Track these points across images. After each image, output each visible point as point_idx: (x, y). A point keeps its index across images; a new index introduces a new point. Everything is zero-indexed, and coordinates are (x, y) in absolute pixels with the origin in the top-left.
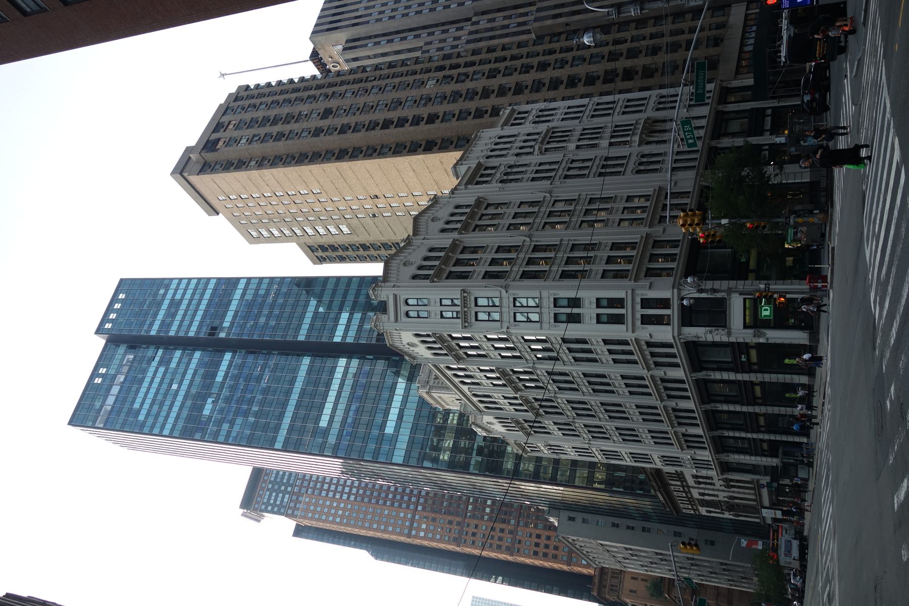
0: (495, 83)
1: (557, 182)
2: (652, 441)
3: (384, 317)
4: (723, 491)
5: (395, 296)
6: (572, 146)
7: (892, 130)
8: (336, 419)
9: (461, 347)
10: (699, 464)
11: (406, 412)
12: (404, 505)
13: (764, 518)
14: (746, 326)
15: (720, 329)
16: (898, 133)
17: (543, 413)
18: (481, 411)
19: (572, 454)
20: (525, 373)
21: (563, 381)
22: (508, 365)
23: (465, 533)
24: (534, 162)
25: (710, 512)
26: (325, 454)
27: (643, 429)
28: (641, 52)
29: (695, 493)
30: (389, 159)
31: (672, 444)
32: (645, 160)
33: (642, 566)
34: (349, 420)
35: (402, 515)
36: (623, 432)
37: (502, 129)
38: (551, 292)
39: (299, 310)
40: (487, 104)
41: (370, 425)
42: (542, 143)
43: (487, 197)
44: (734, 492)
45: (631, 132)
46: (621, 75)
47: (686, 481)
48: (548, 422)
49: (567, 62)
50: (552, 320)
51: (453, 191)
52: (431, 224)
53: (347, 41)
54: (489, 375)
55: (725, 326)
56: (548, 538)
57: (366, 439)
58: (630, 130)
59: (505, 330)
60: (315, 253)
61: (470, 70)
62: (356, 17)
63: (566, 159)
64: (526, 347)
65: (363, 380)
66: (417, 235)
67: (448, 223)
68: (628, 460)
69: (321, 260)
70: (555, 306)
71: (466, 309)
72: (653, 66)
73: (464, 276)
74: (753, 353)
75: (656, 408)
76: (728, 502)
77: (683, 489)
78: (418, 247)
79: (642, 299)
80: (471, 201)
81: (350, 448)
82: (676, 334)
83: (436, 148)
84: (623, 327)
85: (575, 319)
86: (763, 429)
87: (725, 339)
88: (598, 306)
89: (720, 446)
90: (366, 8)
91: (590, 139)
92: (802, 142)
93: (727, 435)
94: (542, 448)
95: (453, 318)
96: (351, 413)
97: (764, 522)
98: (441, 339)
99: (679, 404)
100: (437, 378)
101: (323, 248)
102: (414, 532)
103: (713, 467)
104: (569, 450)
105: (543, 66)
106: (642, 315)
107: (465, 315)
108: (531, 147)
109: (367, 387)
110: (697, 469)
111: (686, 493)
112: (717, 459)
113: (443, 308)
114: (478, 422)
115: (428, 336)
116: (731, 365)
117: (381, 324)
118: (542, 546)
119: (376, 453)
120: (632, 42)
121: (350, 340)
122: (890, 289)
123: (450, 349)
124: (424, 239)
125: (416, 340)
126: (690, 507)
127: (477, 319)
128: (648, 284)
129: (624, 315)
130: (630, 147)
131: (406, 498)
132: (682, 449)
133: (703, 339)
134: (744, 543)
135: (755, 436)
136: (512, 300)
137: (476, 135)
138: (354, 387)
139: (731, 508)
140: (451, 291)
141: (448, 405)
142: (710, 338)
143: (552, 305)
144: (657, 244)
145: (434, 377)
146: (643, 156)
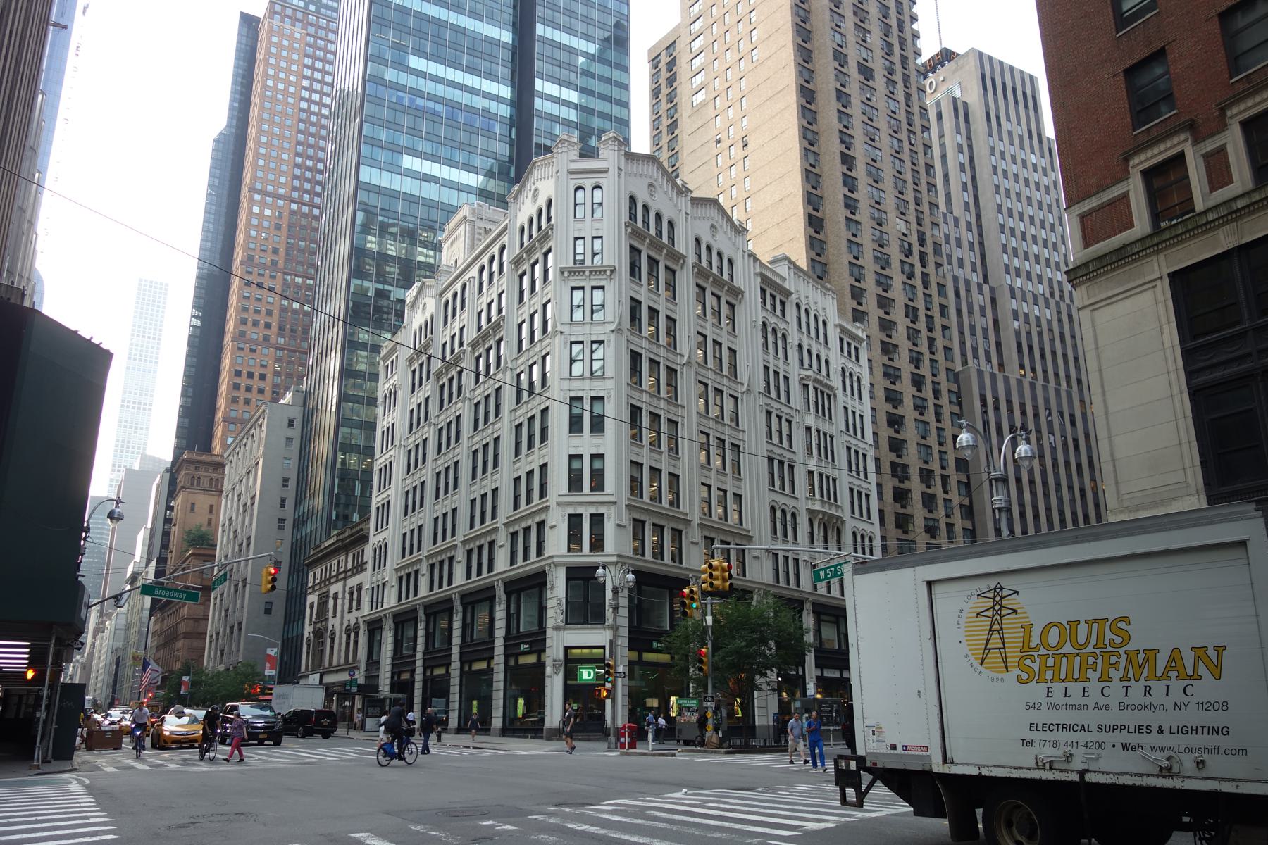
0: (898, 315)
1: (762, 401)
2: (407, 530)
3: (575, 153)
4: (342, 624)
5: (605, 171)
6: (810, 421)
7: (843, 819)
8: (421, 81)
9: (533, 266)
10: (378, 592)
11: (435, 187)
12: (296, 183)
13: (308, 676)
14: (567, 649)
15: (563, 617)
16: (840, 828)
17: (441, 383)
18: (441, 294)
19: (385, 423)
20: (498, 358)
21: (487, 410)
22: (509, 333)
23: (262, 272)
24: (790, 369)
25: (312, 608)
26: (369, 63)
27: (424, 518)
28: (931, 511)
29: (336, 588)
30: (799, 163)
31: (403, 556)
32: (789, 517)
33: (230, 519)
34: (420, 102)
35: (283, 180)
36: (418, 491)
37: (836, 326)
38: (613, 393)
39: (581, 27)
40: (870, 305)
41: (414, 132)
42: (816, 380)
43: (743, 302)
44: (341, 637)
45: (825, 499)
46: (901, 485)
47: (353, 575)
48: (429, 389)
49: (922, 414)
50: (573, 394)
51: (752, 255)
52: (708, 224)
53: (965, 104)
54: (494, 306)
55: (567, 623)
56: (261, 391)
57: (394, 126)
58: (829, 498)
59: (559, 329)
60: (664, 53)
61: (918, 281)
62: (998, 118)
63: (793, 413)
64: (535, 359)
65: (479, 122)
66: (692, 204)
67: (709, 248)
68: (379, 498)
69: (655, 62)
70: (593, 398)
71: (587, 273)
72: (911, 527)
73: (634, 270)
74: (532, 659)
75: (453, 535)
76: (326, 629)
78: (676, 206)
79: (602, 515)
80: (739, 282)
81: (379, 102)
82: (555, 560)
83: (812, 232)
84: (564, 488)
85: (575, 425)
86: (428, 673)
87: (550, 623)
88: (593, 457)
89: (404, 620)
90: (1010, 133)
91: (819, 445)
92: (807, 715)
93: (419, 627)
94: (391, 382)
95: (575, 254)
96: (430, 104)
97: (301, 677)
98: (544, 237)
99: (460, 565)
100: (487, 231)
101: (672, 64)
102: (257, 197)
103: (374, 611)
104: (390, 419)
105: (918, 382)
106: (581, 515)
107: (579, 272)
108: (811, 366)
109: (470, 128)
111: (336, 576)
112: (385, 615)
113: (588, 240)
114: (425, 291)
115: (549, 219)
116: (515, 632)
117: (565, 150)
118: (249, 382)
119: (374, 142)
120: (945, 500)
121: (538, 103)
122: (639, 821)
123: (530, 250)
124: (687, 214)
125: (542, 202)
126: (317, 581)
127: (573, 288)
128: (623, 523)
129: (582, 490)
130: (807, 498)
131: (307, 186)
132: (397, 570)
133: (549, 595)
134: (273, 652)
135: (419, 663)
136: (601, 338)
137: (828, 289)
138: (470, 109)
139: (319, 634)
140: (613, 253)
141: (449, 247)
142: (550, 604)
143: (594, 394)
144: (677, 534)
145: (488, 228)
146: (794, 515)
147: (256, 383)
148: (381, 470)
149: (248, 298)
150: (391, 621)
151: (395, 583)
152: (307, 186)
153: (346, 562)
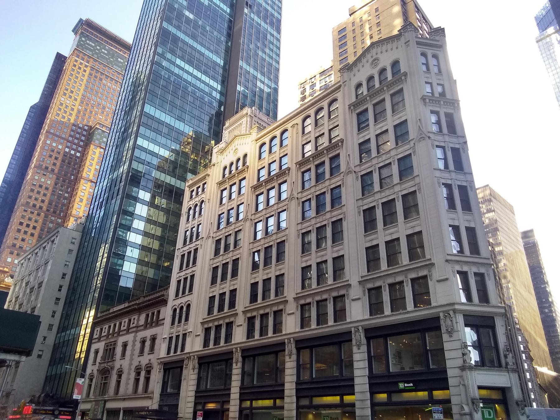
4: (131, 364)
12: (72, 133)
23: (45, 173)
26: (156, 56)
29: (129, 338)
33: (17, 298)
35: (65, 130)
44: (129, 374)
56: (32, 235)
77: (133, 328)
82: (457, 307)
102: (50, 136)
107: (436, 101)
118: (27, 229)
131: (78, 136)
147: (30, 230)
148: (183, 256)
149: (35, 185)
150: (196, 361)
151: (200, 331)
152: (78, 136)
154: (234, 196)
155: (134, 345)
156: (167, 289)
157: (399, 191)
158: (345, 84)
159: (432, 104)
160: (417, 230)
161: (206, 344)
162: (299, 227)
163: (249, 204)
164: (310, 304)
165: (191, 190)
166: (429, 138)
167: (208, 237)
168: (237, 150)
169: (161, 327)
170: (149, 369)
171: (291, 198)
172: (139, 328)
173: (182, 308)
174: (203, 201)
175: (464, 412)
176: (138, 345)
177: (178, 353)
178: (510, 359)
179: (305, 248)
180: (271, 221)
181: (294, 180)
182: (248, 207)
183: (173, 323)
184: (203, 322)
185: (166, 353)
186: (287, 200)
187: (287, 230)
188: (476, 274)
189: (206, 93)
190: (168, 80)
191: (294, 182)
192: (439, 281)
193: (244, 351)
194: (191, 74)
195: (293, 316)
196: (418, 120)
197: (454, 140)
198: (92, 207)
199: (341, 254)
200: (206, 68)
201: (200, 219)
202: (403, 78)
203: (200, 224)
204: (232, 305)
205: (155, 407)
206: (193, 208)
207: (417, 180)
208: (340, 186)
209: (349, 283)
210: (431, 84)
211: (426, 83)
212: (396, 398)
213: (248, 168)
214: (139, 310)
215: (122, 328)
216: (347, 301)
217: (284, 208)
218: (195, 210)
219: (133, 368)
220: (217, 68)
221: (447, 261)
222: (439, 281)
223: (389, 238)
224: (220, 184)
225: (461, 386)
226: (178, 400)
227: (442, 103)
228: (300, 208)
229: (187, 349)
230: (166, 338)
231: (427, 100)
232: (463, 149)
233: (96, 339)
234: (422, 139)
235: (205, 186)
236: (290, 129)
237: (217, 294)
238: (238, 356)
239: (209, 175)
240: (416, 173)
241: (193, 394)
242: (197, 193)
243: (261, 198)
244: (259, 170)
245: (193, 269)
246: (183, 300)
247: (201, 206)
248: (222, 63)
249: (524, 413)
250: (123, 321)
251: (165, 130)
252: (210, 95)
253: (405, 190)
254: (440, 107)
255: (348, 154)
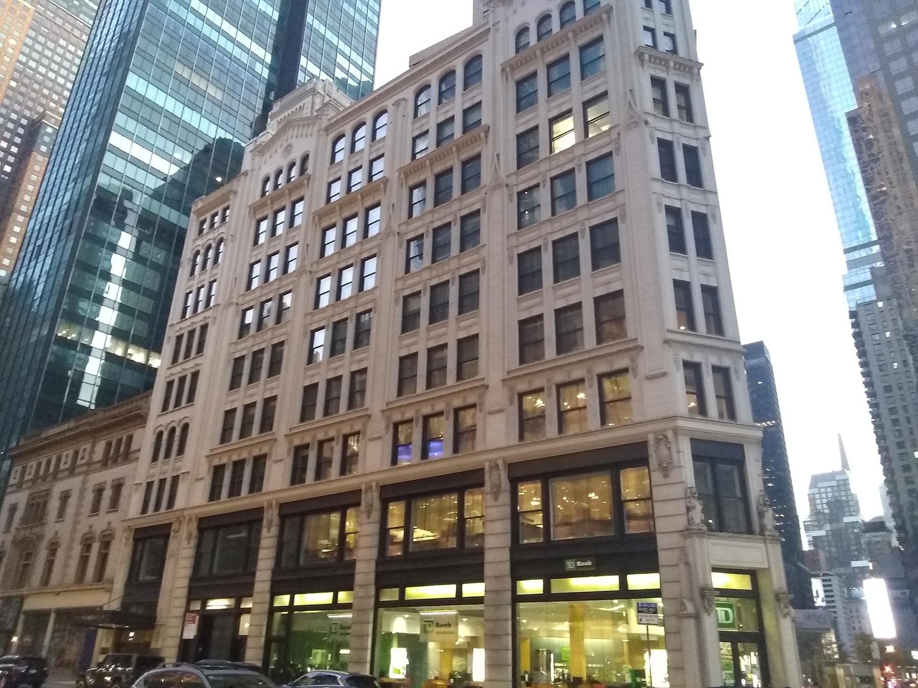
2: (321, 378)
4: (74, 531)
29: (73, 484)
77: (82, 465)
82: (681, 423)
110: (145, 485)
148: (179, 338)
151: (205, 472)
153: (92, 452)
154: (280, 230)
155: (81, 497)
156: (148, 397)
157: (586, 219)
158: (497, 26)
159: (653, 65)
160: (615, 287)
161: (214, 495)
162: (400, 285)
163: (308, 245)
164: (410, 421)
165: (202, 218)
166: (646, 123)
167: (229, 304)
168: (289, 148)
169: (133, 465)
170: (107, 539)
171: (386, 234)
172: (94, 467)
173: (173, 430)
174: (221, 241)
175: (685, 613)
176: (90, 497)
177: (162, 510)
178: (769, 519)
179: (409, 322)
180: (349, 276)
181: (394, 200)
182: (305, 250)
183: (155, 458)
184: (210, 455)
185: (140, 511)
186: (380, 237)
187: (378, 291)
188: (716, 369)
189: (244, 66)
190: (173, 35)
191: (393, 205)
192: (649, 378)
193: (282, 506)
194: (219, 30)
195: (379, 442)
196: (628, 93)
197: (688, 132)
198: (22, 254)
199: (472, 332)
200: (245, 21)
201: (215, 272)
202: (604, 16)
203: (215, 281)
204: (267, 424)
205: (115, 606)
206: (202, 252)
207: (620, 199)
208: (478, 211)
209: (486, 382)
210: (652, 31)
211: (646, 28)
212: (558, 586)
213: (309, 179)
214: (94, 434)
215: (62, 467)
216: (479, 415)
217: (373, 252)
218: (206, 254)
219: (78, 537)
220: (266, 23)
221: (667, 342)
222: (649, 378)
223: (561, 304)
224: (255, 209)
225: (682, 566)
226: (156, 594)
227: (672, 64)
228: (403, 251)
229: (179, 503)
230: (140, 484)
231: (647, 57)
232: (704, 149)
233: (12, 486)
234: (633, 126)
235: (228, 212)
236: (390, 109)
237: (239, 406)
238: (271, 516)
239: (235, 193)
240: (618, 183)
241: (185, 583)
242: (212, 225)
243: (332, 235)
244: (330, 185)
245: (198, 361)
246: (175, 417)
247: (218, 248)
248: (276, 16)
249: (787, 614)
250: (65, 454)
251: (163, 123)
252: (252, 70)
253: (598, 218)
254: (668, 72)
255: (496, 153)
